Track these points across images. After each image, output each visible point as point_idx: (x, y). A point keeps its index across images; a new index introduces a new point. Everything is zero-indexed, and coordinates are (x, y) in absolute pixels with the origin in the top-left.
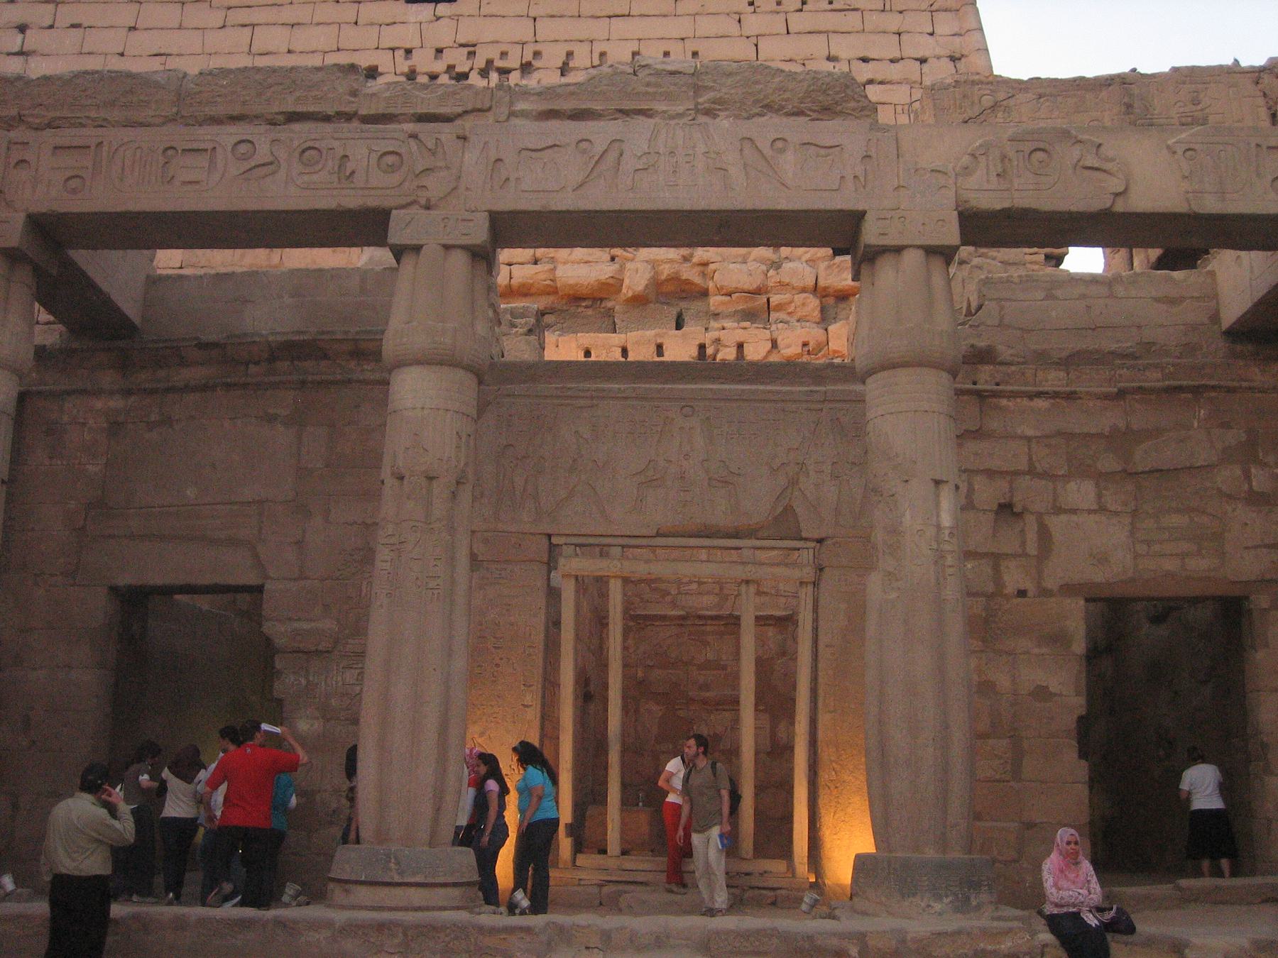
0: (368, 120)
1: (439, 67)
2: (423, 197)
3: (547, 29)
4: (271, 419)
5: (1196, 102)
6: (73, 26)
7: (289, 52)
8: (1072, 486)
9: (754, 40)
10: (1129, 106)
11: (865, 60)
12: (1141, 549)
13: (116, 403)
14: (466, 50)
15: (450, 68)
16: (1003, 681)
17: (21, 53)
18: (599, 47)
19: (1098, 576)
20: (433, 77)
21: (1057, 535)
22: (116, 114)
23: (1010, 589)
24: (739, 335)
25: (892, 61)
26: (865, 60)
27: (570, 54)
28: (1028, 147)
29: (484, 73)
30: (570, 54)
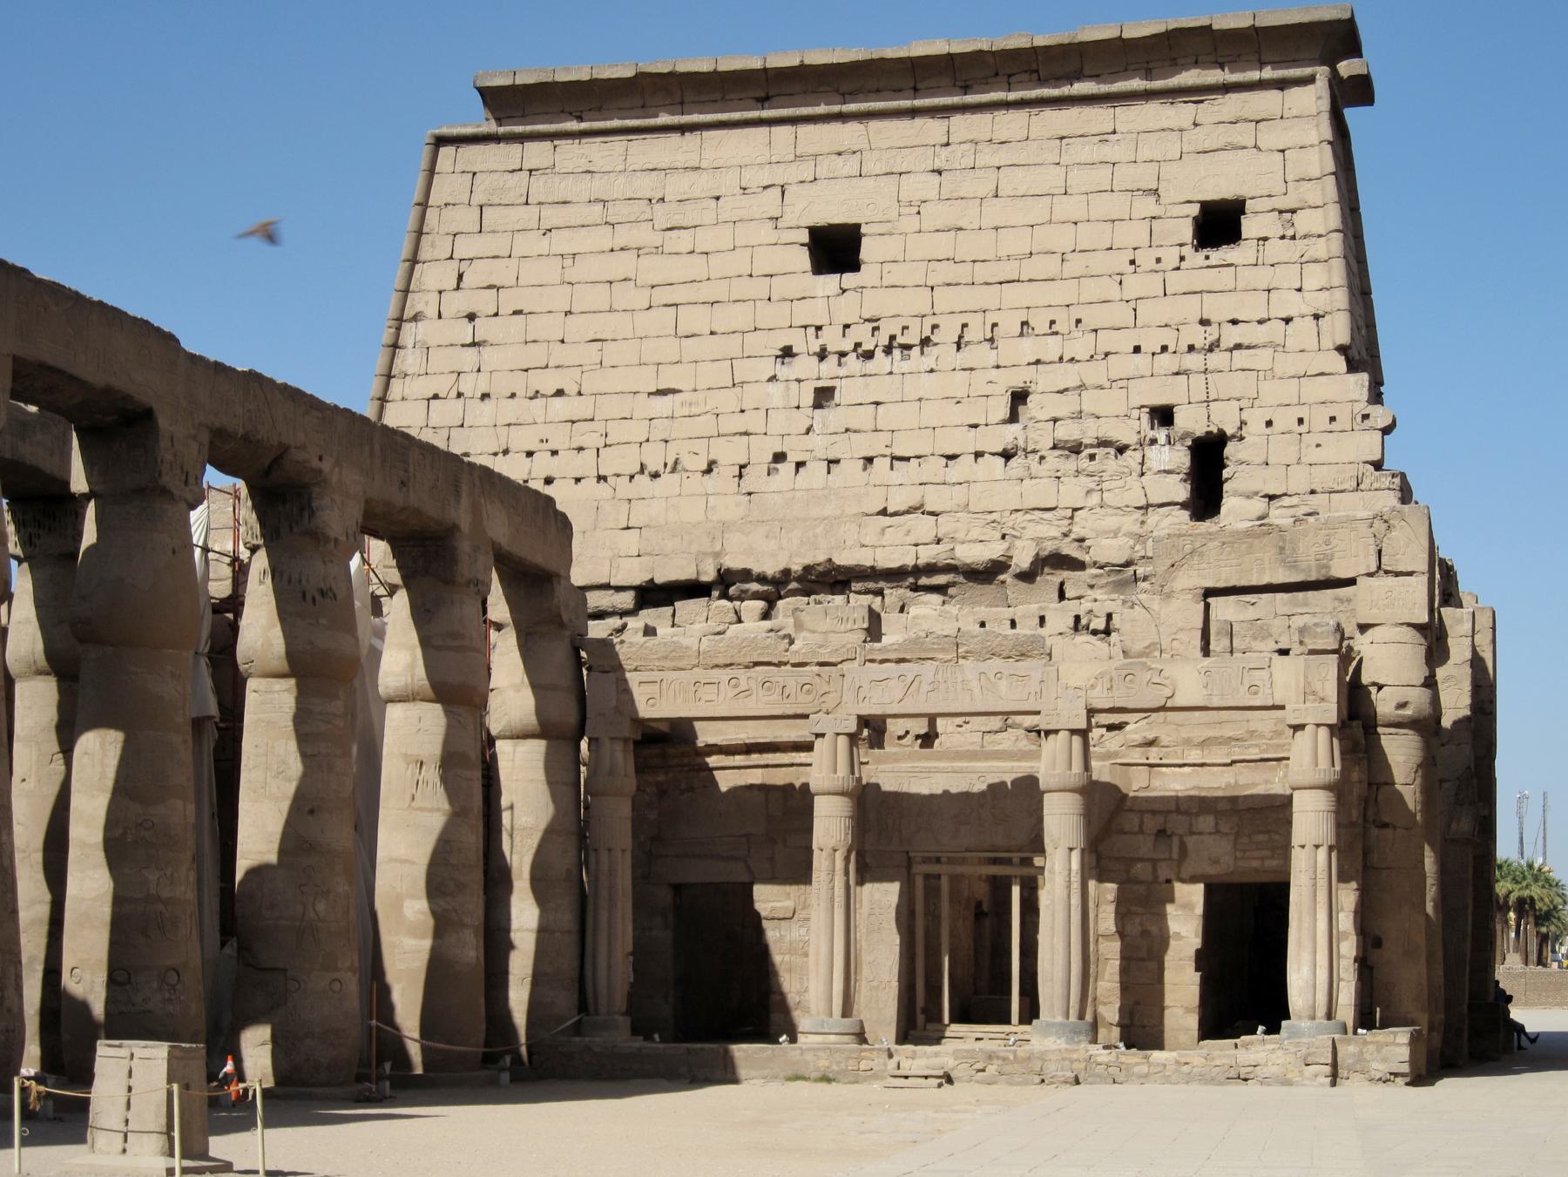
0: (794, 665)
1: (847, 345)
2: (824, 707)
3: (945, 299)
6: (516, 313)
7: (712, 333)
8: (1201, 819)
9: (1132, 304)
10: (1282, 549)
11: (1234, 322)
12: (1239, 854)
13: (661, 778)
14: (870, 326)
15: (858, 345)
17: (474, 344)
18: (991, 318)
19: (1212, 870)
20: (843, 354)
21: (1190, 846)
22: (668, 664)
23: (1162, 878)
24: (1110, 607)
25: (1260, 322)
26: (1234, 322)
27: (964, 326)
28: (1124, 672)
30: (964, 326)
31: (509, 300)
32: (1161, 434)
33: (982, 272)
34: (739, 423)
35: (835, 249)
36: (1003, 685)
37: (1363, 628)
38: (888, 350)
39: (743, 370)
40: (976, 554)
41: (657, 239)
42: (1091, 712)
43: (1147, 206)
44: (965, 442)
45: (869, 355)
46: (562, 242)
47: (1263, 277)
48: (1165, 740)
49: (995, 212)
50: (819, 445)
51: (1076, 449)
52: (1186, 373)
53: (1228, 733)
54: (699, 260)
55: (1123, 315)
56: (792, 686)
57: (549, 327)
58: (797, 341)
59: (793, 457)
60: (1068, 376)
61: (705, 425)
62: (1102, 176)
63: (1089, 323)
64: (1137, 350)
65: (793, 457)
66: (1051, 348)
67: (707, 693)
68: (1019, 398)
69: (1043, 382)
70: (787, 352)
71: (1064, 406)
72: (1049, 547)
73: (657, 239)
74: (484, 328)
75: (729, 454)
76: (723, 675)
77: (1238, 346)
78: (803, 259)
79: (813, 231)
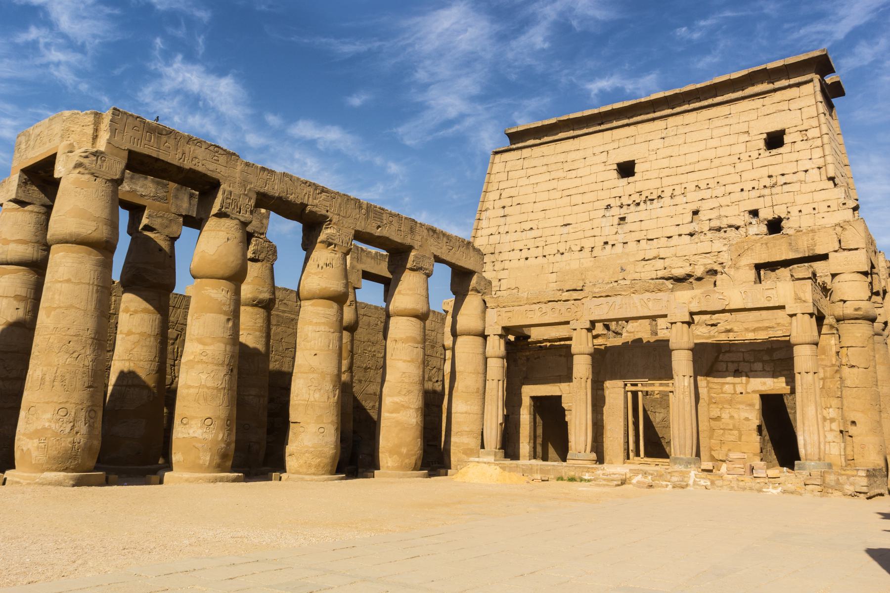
1: (630, 202)
3: (666, 182)
4: (561, 356)
5: (813, 239)
11: (783, 175)
13: (528, 353)
16: (736, 416)
20: (629, 205)
23: (738, 392)
26: (783, 175)
29: (645, 202)
31: (516, 201)
32: (754, 221)
33: (680, 170)
34: (592, 233)
35: (626, 169)
36: (650, 304)
37: (834, 276)
38: (645, 202)
39: (593, 215)
40: (679, 272)
41: (565, 174)
42: (692, 314)
43: (745, 137)
44: (674, 231)
45: (638, 204)
46: (533, 180)
47: (795, 156)
48: (736, 329)
49: (685, 149)
50: (621, 238)
51: (719, 229)
52: (763, 196)
53: (766, 324)
54: (578, 180)
55: (737, 178)
56: (563, 309)
57: (530, 207)
58: (612, 202)
59: (610, 243)
60: (714, 203)
61: (580, 235)
62: (726, 130)
63: (722, 182)
64: (742, 190)
65: (610, 243)
66: (706, 194)
67: (530, 315)
68: (696, 213)
69: (704, 206)
70: (608, 207)
71: (713, 214)
72: (709, 267)
73: (565, 174)
74: (507, 211)
75: (588, 244)
76: (537, 307)
77: (785, 184)
78: (615, 174)
79: (618, 164)
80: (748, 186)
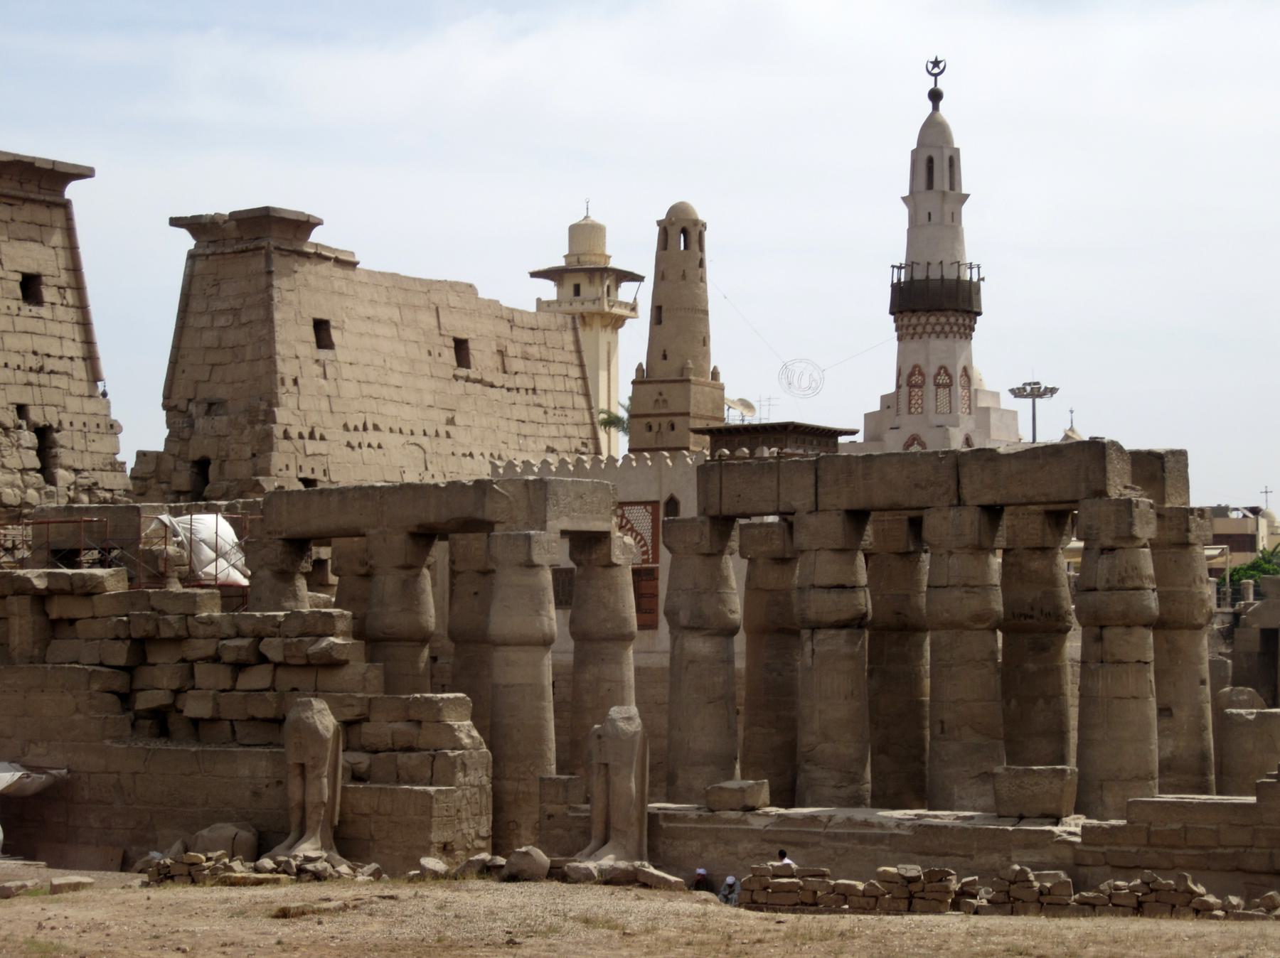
25: (61, 358)
26: (49, 356)
47: (55, 329)
52: (29, 384)
77: (52, 372)
80: (12, 364)
